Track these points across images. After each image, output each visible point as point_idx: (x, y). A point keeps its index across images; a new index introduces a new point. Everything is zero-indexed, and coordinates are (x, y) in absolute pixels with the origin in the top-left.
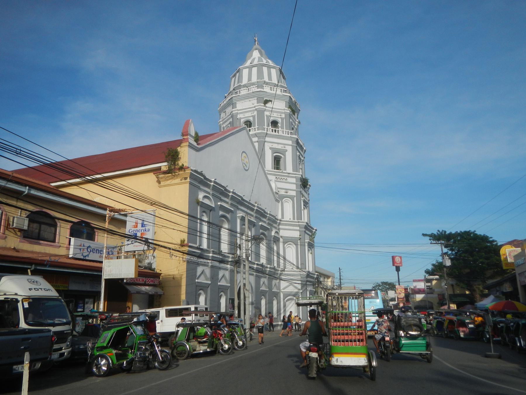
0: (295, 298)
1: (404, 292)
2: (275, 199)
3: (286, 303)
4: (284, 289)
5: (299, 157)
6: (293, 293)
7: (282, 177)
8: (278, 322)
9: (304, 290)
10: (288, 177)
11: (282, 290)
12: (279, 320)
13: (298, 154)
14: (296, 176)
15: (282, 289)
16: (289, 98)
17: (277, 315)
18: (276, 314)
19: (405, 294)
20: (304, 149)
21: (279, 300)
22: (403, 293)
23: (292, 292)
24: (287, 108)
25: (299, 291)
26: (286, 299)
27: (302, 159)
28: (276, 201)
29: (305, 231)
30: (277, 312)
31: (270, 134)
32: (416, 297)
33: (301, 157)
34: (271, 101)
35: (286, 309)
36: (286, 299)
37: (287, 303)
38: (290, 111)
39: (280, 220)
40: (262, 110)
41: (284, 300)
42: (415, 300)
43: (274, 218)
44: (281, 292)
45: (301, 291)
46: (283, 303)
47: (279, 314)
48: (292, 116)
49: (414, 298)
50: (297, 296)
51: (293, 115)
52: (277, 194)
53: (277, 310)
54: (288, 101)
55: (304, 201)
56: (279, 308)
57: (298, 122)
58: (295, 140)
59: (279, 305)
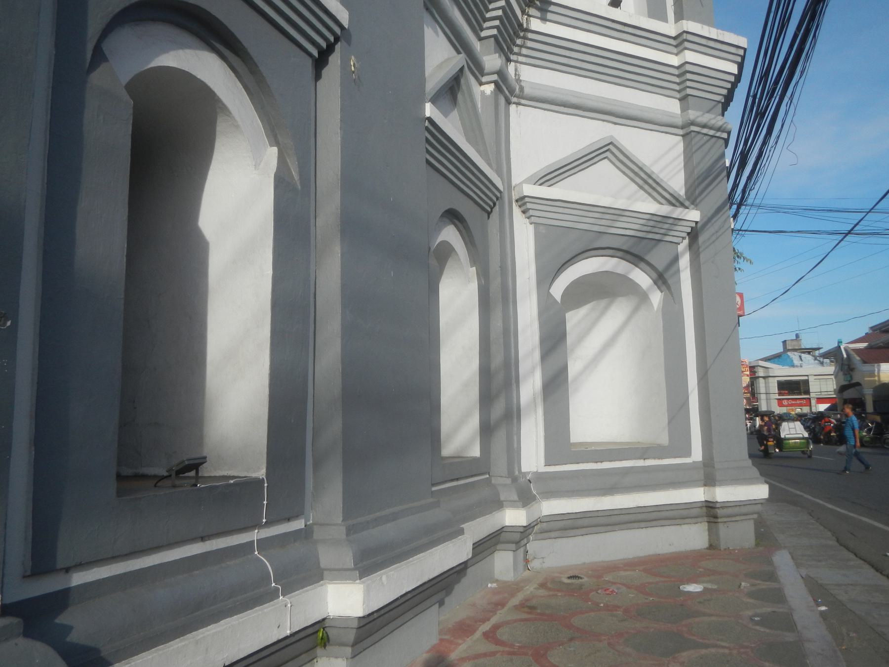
0: (641, 278)
1: (748, 373)
3: (568, 315)
4: (550, 177)
6: (628, 227)
8: (498, 505)
9: (719, 210)
11: (530, 190)
12: (500, 480)
15: (527, 181)
17: (487, 430)
18: (474, 422)
19: (751, 378)
21: (503, 268)
22: (748, 375)
23: (619, 213)
25: (678, 212)
26: (558, 289)
30: (487, 398)
32: (879, 371)
35: (564, 369)
36: (558, 289)
37: (574, 319)
41: (545, 277)
42: (876, 378)
44: (516, 211)
45: (694, 215)
46: (541, 314)
47: (497, 411)
49: (872, 374)
50: (659, 258)
53: (485, 373)
56: (497, 360)
59: (497, 324)
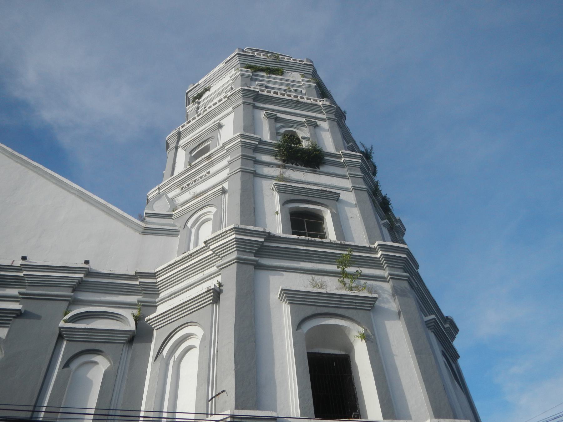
2: (136, 230)
5: (277, 119)
7: (194, 180)
10: (211, 164)
13: (263, 113)
14: (226, 148)
16: (238, 58)
20: (320, 106)
24: (235, 72)
27: (304, 121)
28: (144, 233)
29: (240, 261)
31: (186, 129)
33: (279, 115)
34: (207, 90)
38: (241, 70)
39: (153, 275)
40: (192, 112)
43: (82, 276)
48: (268, 77)
51: (273, 76)
52: (170, 216)
54: (238, 62)
55: (281, 190)
57: (303, 81)
58: (240, 95)
